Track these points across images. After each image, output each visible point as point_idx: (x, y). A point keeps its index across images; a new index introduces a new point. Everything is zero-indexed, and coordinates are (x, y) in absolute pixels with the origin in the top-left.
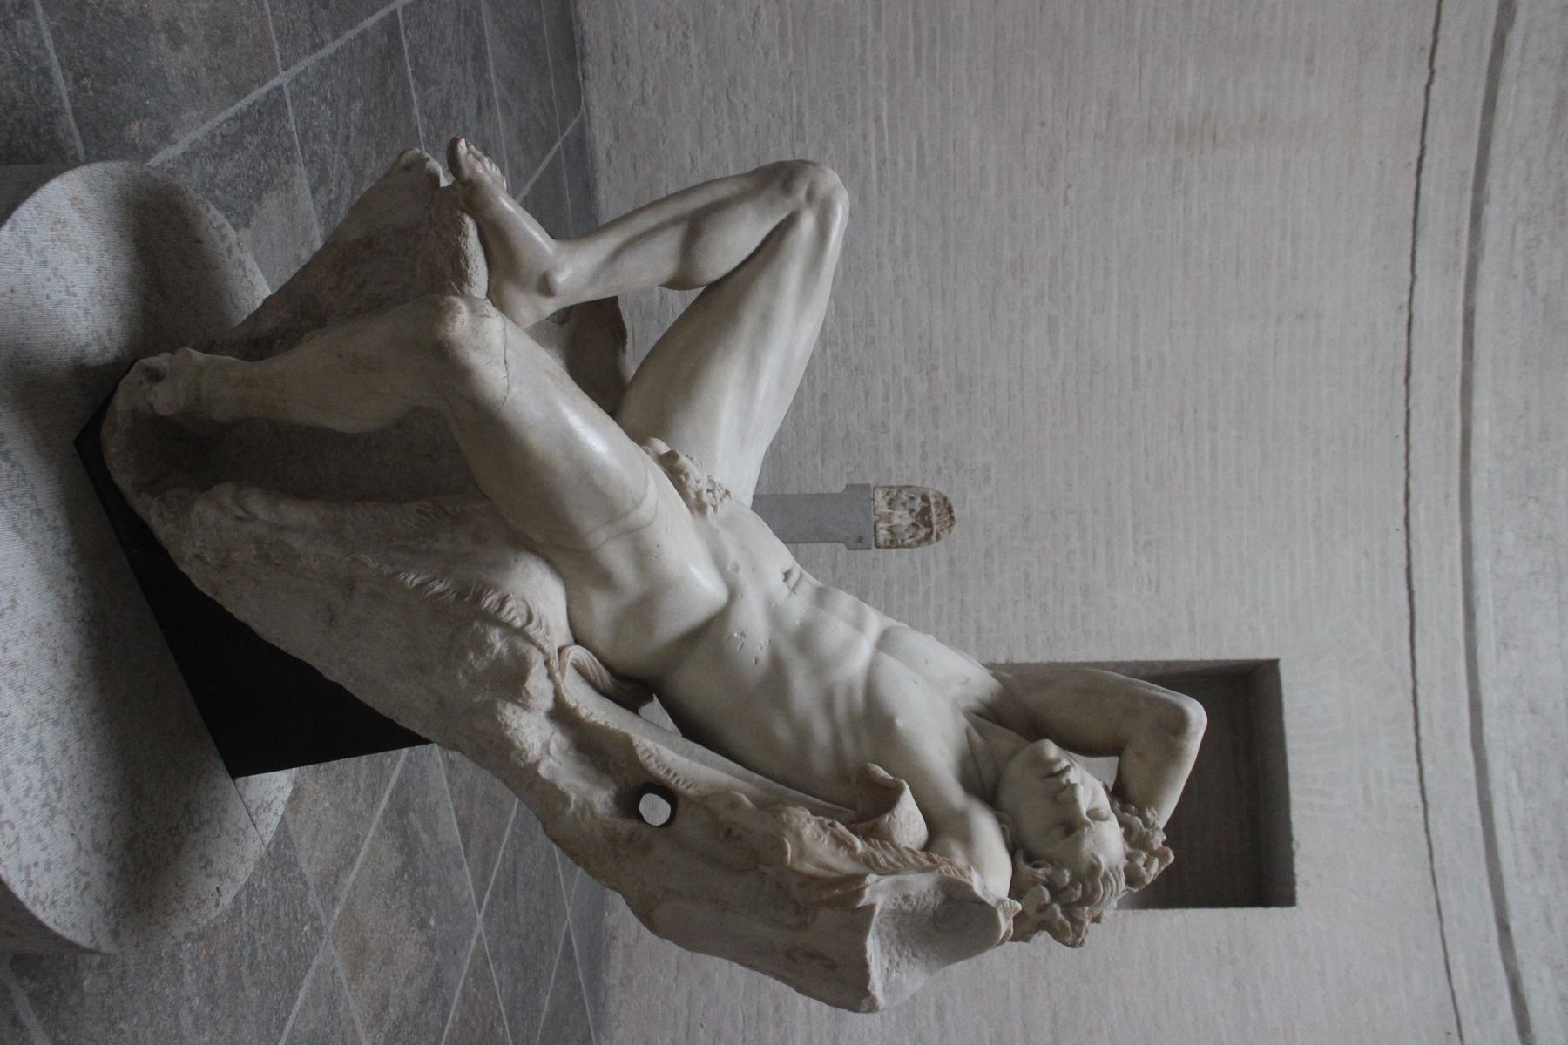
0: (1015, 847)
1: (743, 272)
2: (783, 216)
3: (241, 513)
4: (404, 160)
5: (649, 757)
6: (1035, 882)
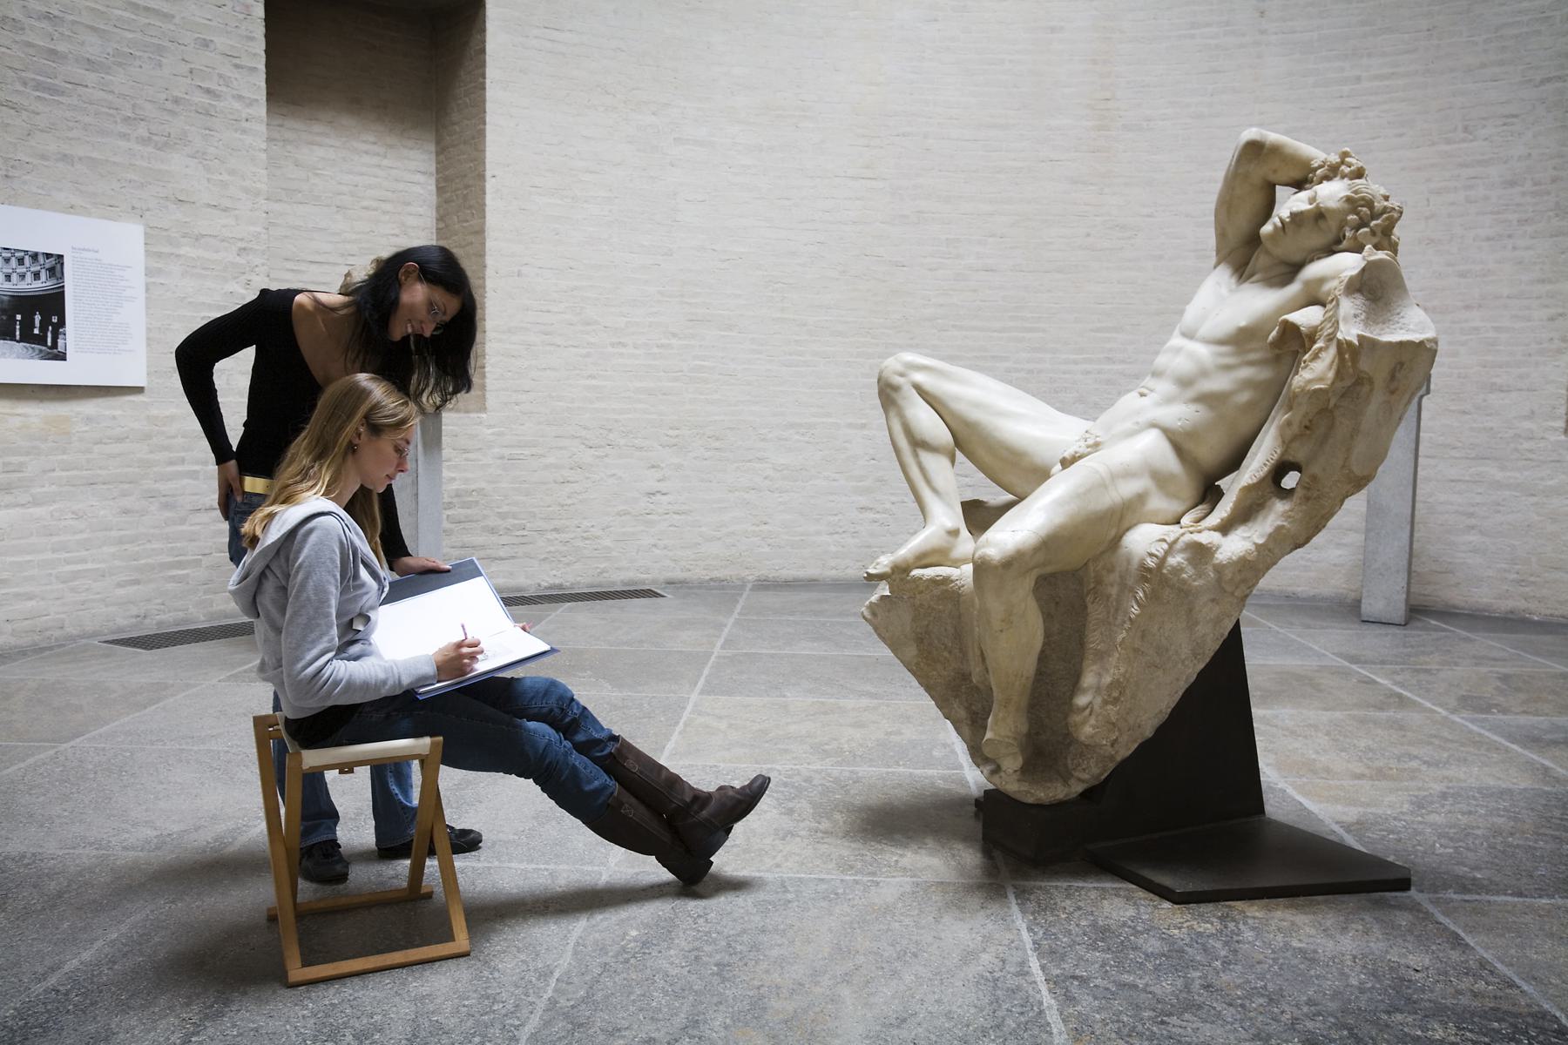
0: (1330, 251)
1: (948, 419)
2: (914, 391)
3: (1088, 711)
4: (869, 617)
6: (1355, 238)
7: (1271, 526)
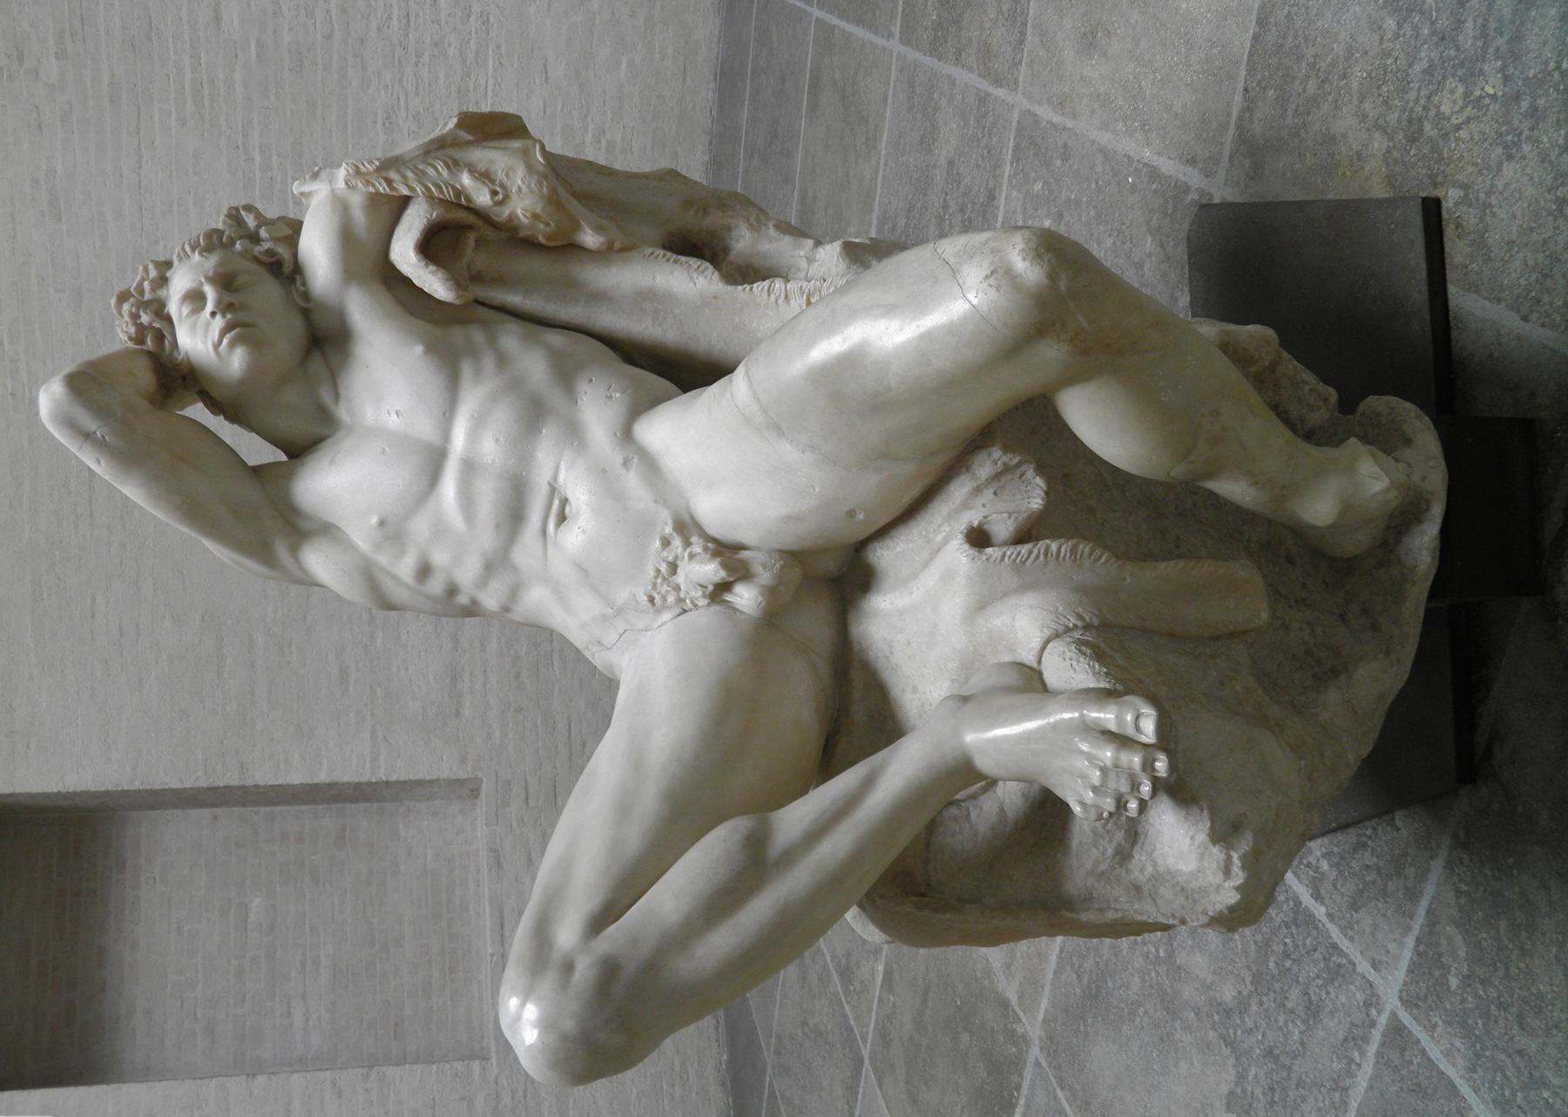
5: (699, 267)
6: (275, 240)
7: (777, 240)
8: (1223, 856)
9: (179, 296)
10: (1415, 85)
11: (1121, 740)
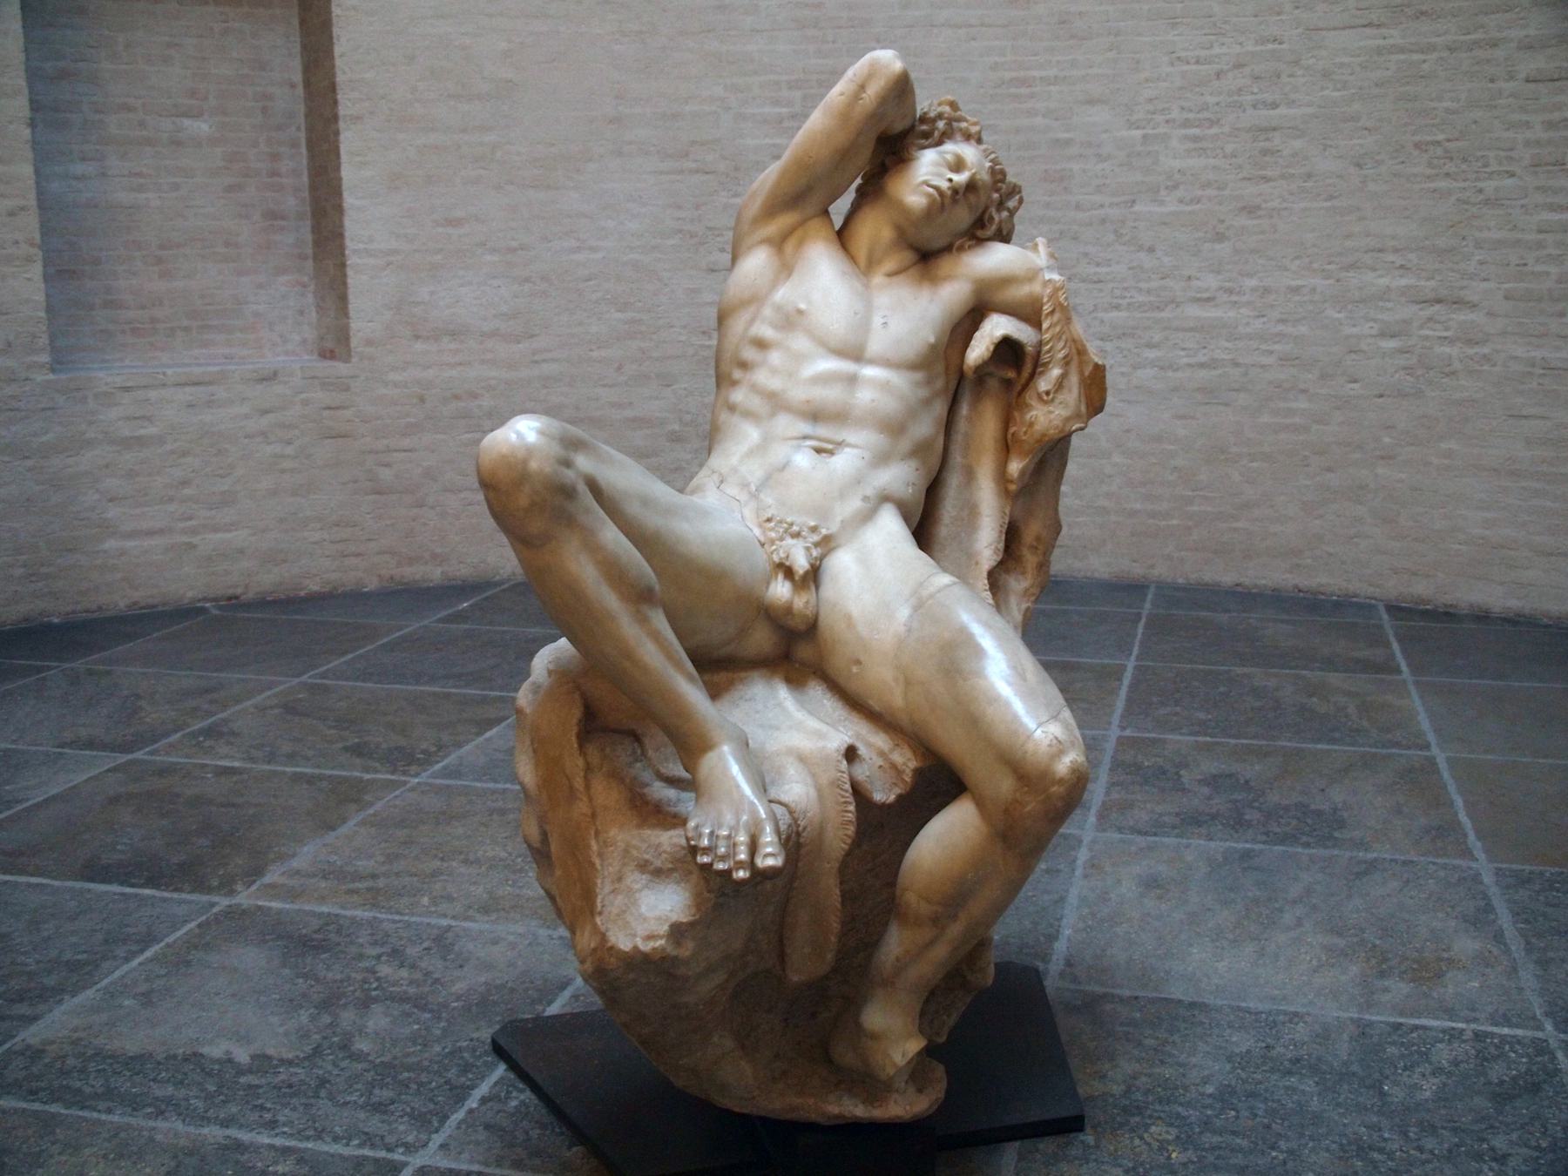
6: (1000, 222)
7: (1019, 610)
8: (662, 933)
9: (960, 152)
10: (1167, 1108)
11: (753, 847)
